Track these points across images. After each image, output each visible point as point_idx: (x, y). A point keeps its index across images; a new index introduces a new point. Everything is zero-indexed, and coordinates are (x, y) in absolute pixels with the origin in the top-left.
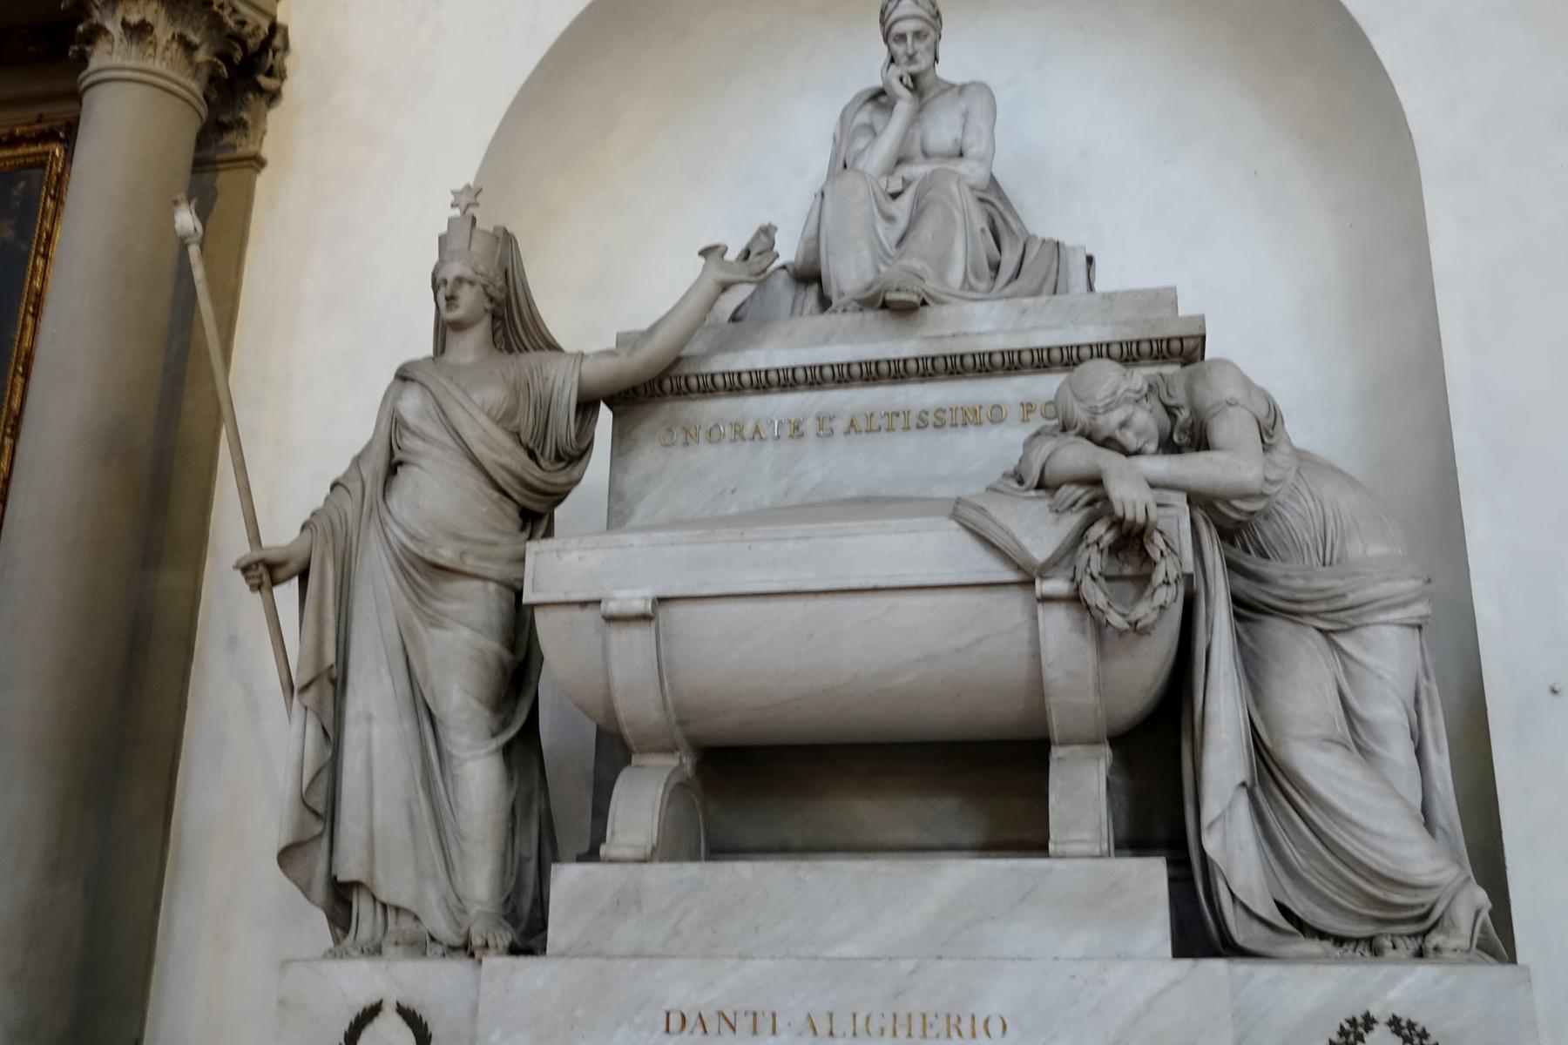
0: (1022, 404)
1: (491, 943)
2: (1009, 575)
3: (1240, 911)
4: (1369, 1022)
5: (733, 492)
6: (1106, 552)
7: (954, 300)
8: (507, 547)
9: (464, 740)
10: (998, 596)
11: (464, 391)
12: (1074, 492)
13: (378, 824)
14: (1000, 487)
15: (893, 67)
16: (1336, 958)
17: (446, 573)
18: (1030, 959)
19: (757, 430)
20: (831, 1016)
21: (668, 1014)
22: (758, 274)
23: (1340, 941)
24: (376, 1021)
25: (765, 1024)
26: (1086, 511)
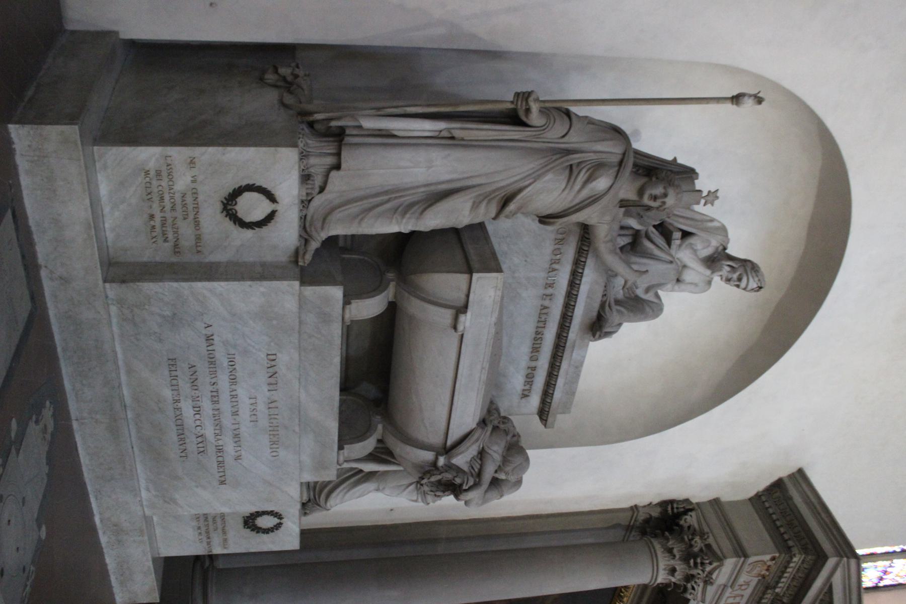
0: (535, 367)
5: (526, 261)
12: (477, 468)
15: (728, 269)
17: (502, 203)
19: (554, 270)
20: (277, 408)
21: (276, 355)
24: (268, 201)
25: (272, 387)
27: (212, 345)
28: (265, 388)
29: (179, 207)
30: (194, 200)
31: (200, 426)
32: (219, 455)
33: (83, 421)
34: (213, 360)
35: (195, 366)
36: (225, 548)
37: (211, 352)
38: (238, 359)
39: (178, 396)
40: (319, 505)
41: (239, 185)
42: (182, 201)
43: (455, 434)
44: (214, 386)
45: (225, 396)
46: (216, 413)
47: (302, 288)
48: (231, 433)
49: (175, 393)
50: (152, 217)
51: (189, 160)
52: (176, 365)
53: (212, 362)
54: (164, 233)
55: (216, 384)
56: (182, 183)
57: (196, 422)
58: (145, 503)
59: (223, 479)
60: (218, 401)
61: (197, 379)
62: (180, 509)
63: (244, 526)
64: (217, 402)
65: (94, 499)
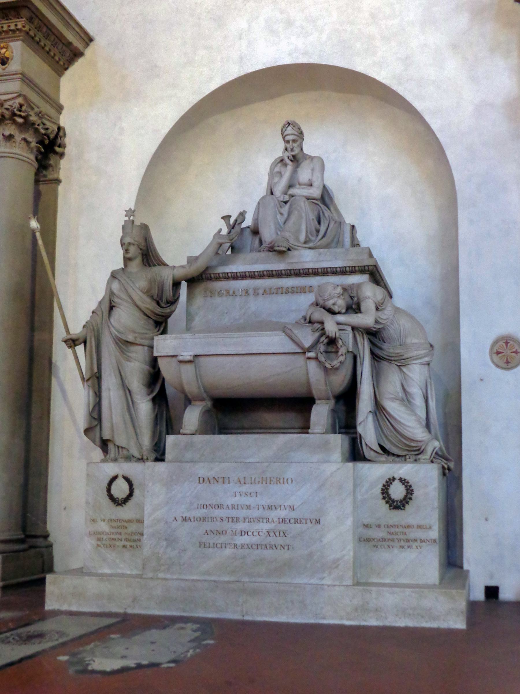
1: (149, 458)
2: (299, 351)
3: (368, 448)
4: (394, 479)
6: (326, 345)
7: (296, 247)
8: (150, 335)
9: (139, 397)
10: (297, 356)
11: (133, 283)
13: (114, 422)
14: (299, 322)
16: (390, 461)
18: (300, 463)
22: (231, 240)
23: (398, 456)
24: (117, 480)
26: (320, 332)
27: (190, 518)
28: (227, 485)
29: (119, 530)
30: (115, 521)
31: (259, 532)
32: (288, 521)
33: (244, 612)
34: (202, 519)
35: (206, 531)
36: (430, 528)
37: (195, 519)
38: (201, 502)
39: (231, 544)
40: (421, 447)
41: (107, 496)
42: (116, 528)
43: (292, 348)
44: (224, 520)
45: (233, 513)
46: (247, 520)
47: (166, 460)
48: (267, 511)
49: (228, 546)
50: (124, 546)
51: (92, 522)
52: (204, 543)
53: (203, 519)
54: (134, 541)
55: (222, 518)
56: (104, 527)
57: (255, 535)
58: (338, 583)
59: (314, 521)
60: (237, 518)
61: (217, 530)
62: (346, 558)
63: (401, 509)
64: (238, 519)
65: (324, 620)
